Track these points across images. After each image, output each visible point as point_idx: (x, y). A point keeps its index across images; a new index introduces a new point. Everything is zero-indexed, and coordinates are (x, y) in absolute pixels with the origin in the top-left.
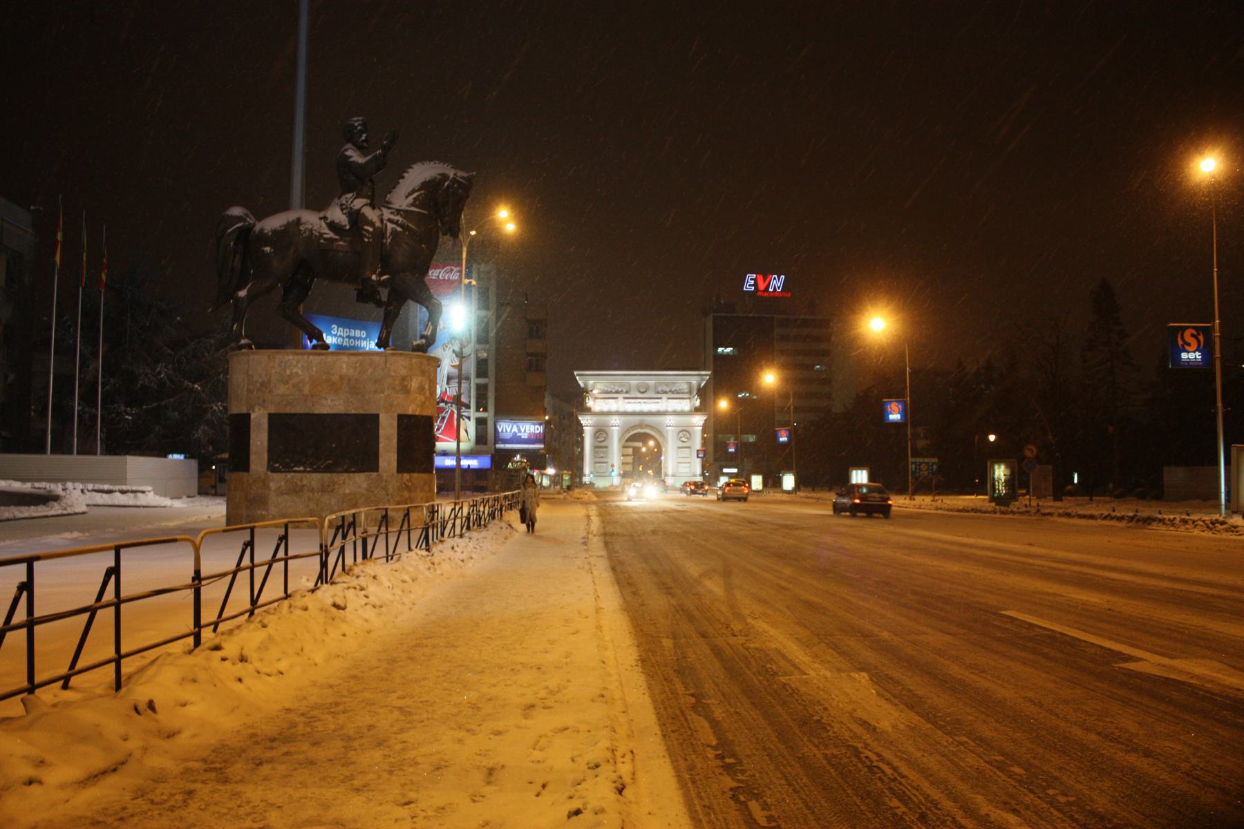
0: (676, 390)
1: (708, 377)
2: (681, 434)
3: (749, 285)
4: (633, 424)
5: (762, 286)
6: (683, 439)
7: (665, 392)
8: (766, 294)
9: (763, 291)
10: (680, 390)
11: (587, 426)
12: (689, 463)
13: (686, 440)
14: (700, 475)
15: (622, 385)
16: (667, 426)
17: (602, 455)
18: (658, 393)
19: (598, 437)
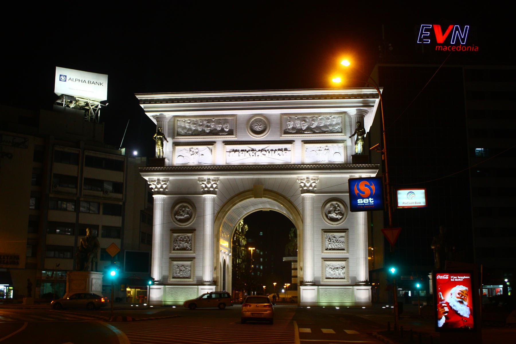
0: (318, 127)
1: (377, 100)
2: (329, 205)
3: (425, 37)
4: (241, 190)
5: (440, 38)
6: (333, 215)
7: (299, 131)
8: (446, 48)
9: (443, 45)
10: (326, 126)
11: (159, 193)
12: (345, 259)
13: (339, 217)
14: (367, 283)
15: (223, 120)
16: (304, 192)
17: (186, 245)
18: (286, 133)
19: (177, 213)
